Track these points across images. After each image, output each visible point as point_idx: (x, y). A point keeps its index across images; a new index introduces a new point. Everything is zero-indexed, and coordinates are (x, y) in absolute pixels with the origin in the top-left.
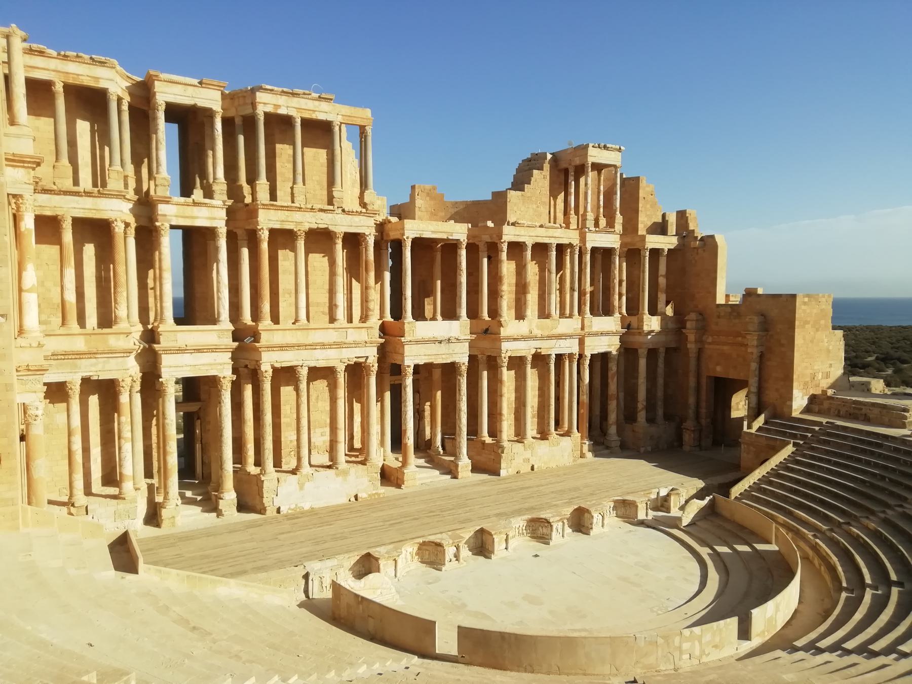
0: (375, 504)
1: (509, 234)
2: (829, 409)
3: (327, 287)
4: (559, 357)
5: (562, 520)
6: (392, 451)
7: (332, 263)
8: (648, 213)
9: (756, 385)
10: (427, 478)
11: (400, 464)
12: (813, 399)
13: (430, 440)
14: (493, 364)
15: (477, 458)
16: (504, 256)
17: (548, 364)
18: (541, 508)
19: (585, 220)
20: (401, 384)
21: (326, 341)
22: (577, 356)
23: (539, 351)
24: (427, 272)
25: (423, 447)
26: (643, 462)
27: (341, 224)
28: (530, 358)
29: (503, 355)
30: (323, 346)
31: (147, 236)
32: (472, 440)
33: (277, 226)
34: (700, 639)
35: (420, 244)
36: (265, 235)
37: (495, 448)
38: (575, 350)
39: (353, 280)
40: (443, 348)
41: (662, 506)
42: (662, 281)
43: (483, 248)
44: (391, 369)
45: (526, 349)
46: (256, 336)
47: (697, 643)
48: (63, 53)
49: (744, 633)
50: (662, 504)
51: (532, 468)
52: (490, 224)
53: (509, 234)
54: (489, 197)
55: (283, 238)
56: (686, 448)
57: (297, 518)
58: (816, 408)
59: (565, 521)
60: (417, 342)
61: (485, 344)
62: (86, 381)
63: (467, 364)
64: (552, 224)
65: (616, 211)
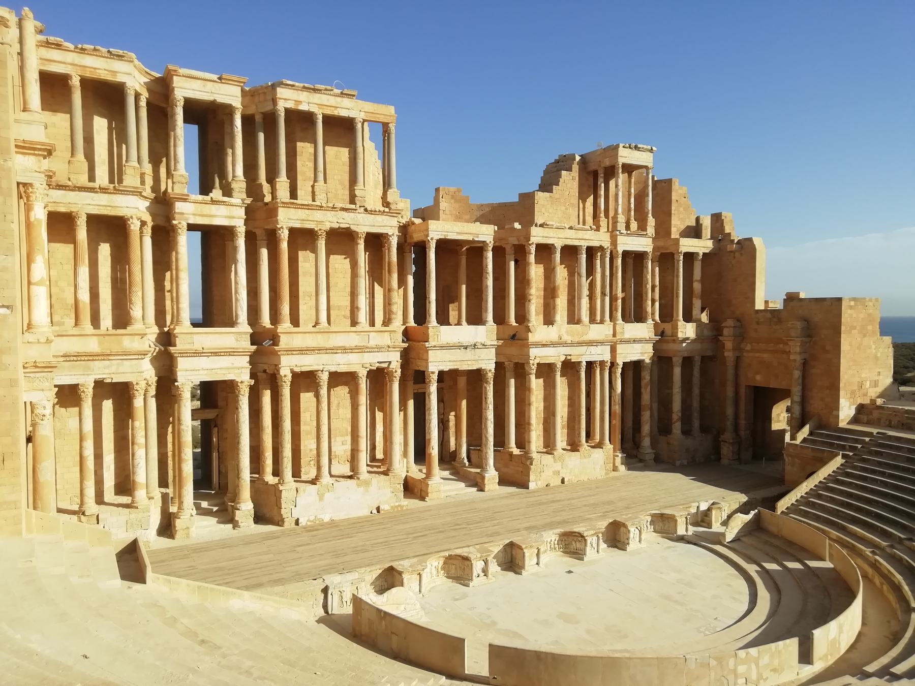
1: (537, 236)
3: (348, 289)
4: (590, 365)
7: (354, 265)
8: (681, 216)
11: (424, 476)
13: (455, 452)
15: (505, 470)
16: (532, 258)
17: (578, 372)
19: (615, 222)
21: (347, 345)
22: (609, 364)
23: (569, 357)
25: (448, 459)
26: (679, 476)
27: (363, 224)
28: (559, 365)
30: (345, 350)
31: (164, 236)
32: (499, 451)
33: (297, 225)
34: (756, 661)
36: (284, 235)
38: (607, 357)
39: (376, 286)
41: (703, 521)
42: (697, 286)
43: (509, 250)
44: (414, 377)
45: (555, 356)
46: (275, 339)
47: (753, 666)
48: (80, 46)
49: (806, 656)
50: (703, 519)
51: (563, 481)
52: (517, 226)
53: (537, 236)
55: (303, 238)
56: (725, 461)
57: (317, 530)
60: (442, 347)
61: (513, 351)
62: (99, 385)
63: (493, 371)
64: (581, 226)
65: (648, 213)
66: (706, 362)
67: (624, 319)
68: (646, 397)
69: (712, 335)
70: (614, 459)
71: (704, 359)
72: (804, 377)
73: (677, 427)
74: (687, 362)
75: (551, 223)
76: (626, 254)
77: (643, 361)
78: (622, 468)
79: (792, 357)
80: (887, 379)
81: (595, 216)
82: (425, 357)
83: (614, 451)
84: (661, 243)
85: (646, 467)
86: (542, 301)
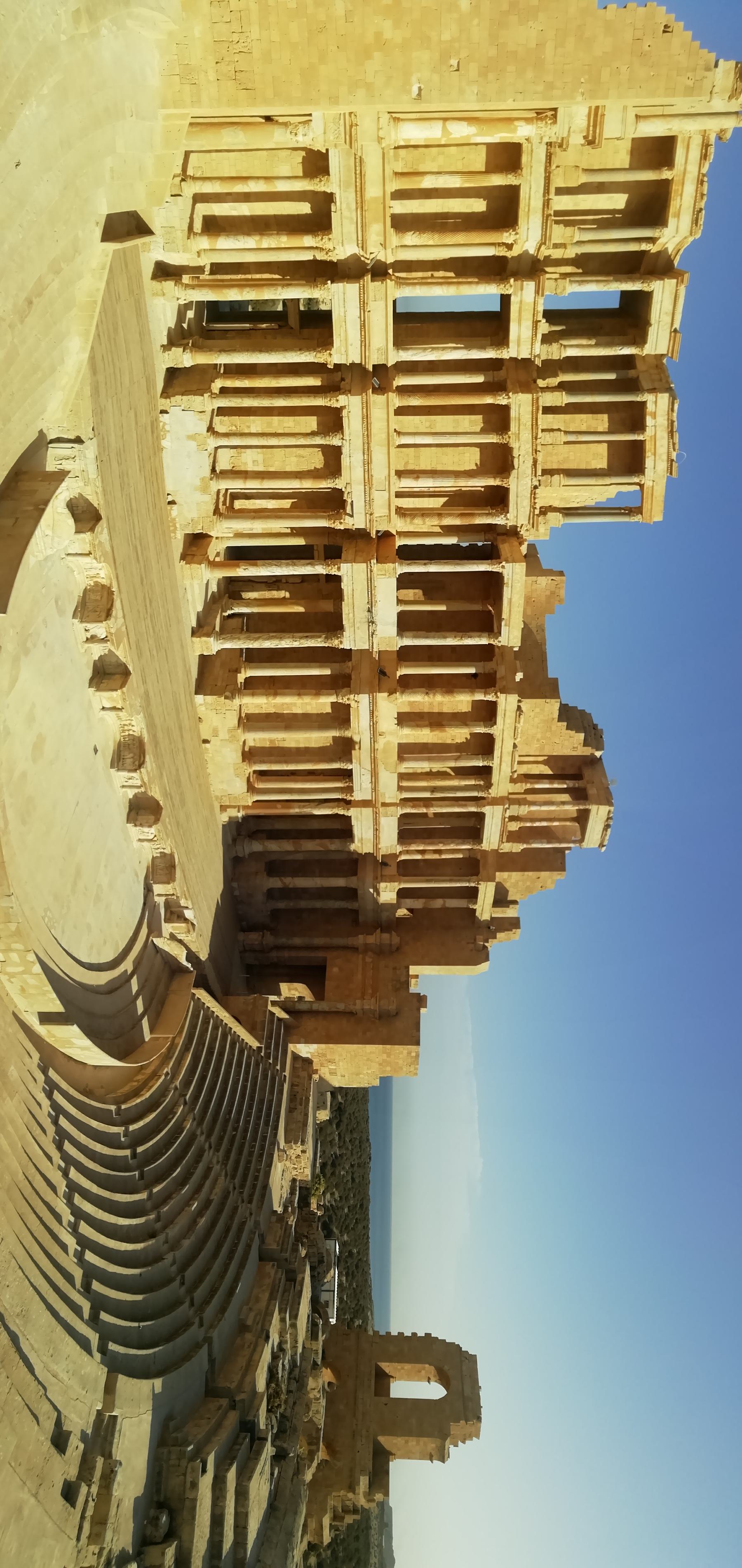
0: (163, 526)
1: (507, 703)
2: (298, 1077)
3: (439, 468)
4: (347, 775)
5: (144, 784)
6: (228, 548)
7: (469, 474)
9: (320, 1009)
10: (193, 596)
11: (211, 559)
12: (308, 1062)
13: (241, 598)
14: (340, 682)
15: (218, 663)
16: (479, 696)
17: (339, 759)
18: (157, 756)
19: (520, 802)
20: (313, 558)
22: (349, 798)
23: (357, 747)
24: (458, 592)
25: (232, 589)
26: (221, 887)
28: (348, 734)
29: (352, 696)
32: (241, 656)
35: (493, 585)
37: (232, 687)
38: (357, 796)
39: (445, 499)
40: (361, 615)
41: (172, 913)
43: (489, 666)
44: (334, 546)
50: (175, 913)
51: (206, 741)
52: (519, 676)
53: (507, 703)
54: (551, 675)
57: (153, 432)
58: (299, 1065)
59: (143, 789)
60: (370, 580)
61: (366, 672)
63: (341, 646)
64: (517, 759)
66: (351, 914)
67: (403, 816)
68: (310, 845)
69: (383, 920)
70: (234, 807)
71: (356, 912)
72: (337, 1013)
73: (275, 883)
74: (352, 894)
75: (522, 720)
76: (481, 817)
77: (353, 841)
78: (224, 818)
79: (358, 1002)
80: (336, 1082)
81: (528, 777)
82: (358, 558)
83: (245, 807)
84: (491, 860)
85: (228, 846)
86: (426, 710)
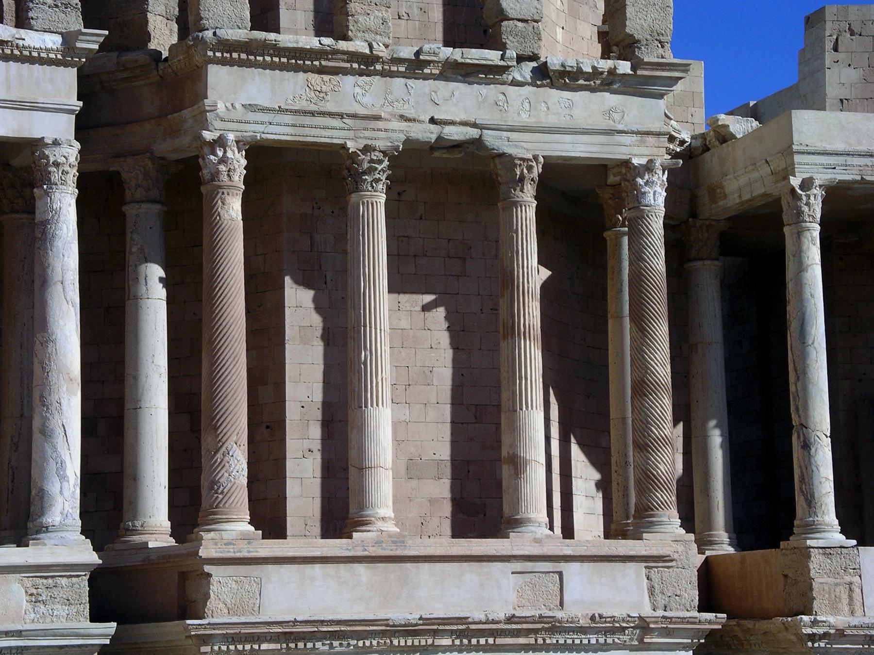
27: (537, 125)
33: (280, 131)
55: (302, 187)
